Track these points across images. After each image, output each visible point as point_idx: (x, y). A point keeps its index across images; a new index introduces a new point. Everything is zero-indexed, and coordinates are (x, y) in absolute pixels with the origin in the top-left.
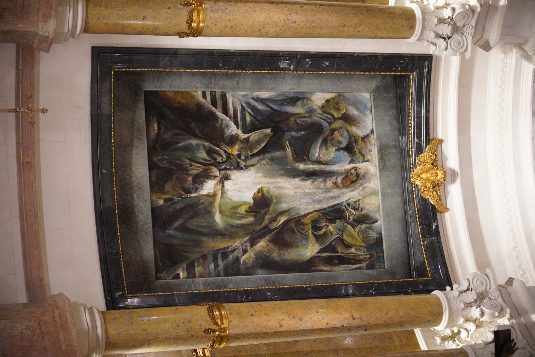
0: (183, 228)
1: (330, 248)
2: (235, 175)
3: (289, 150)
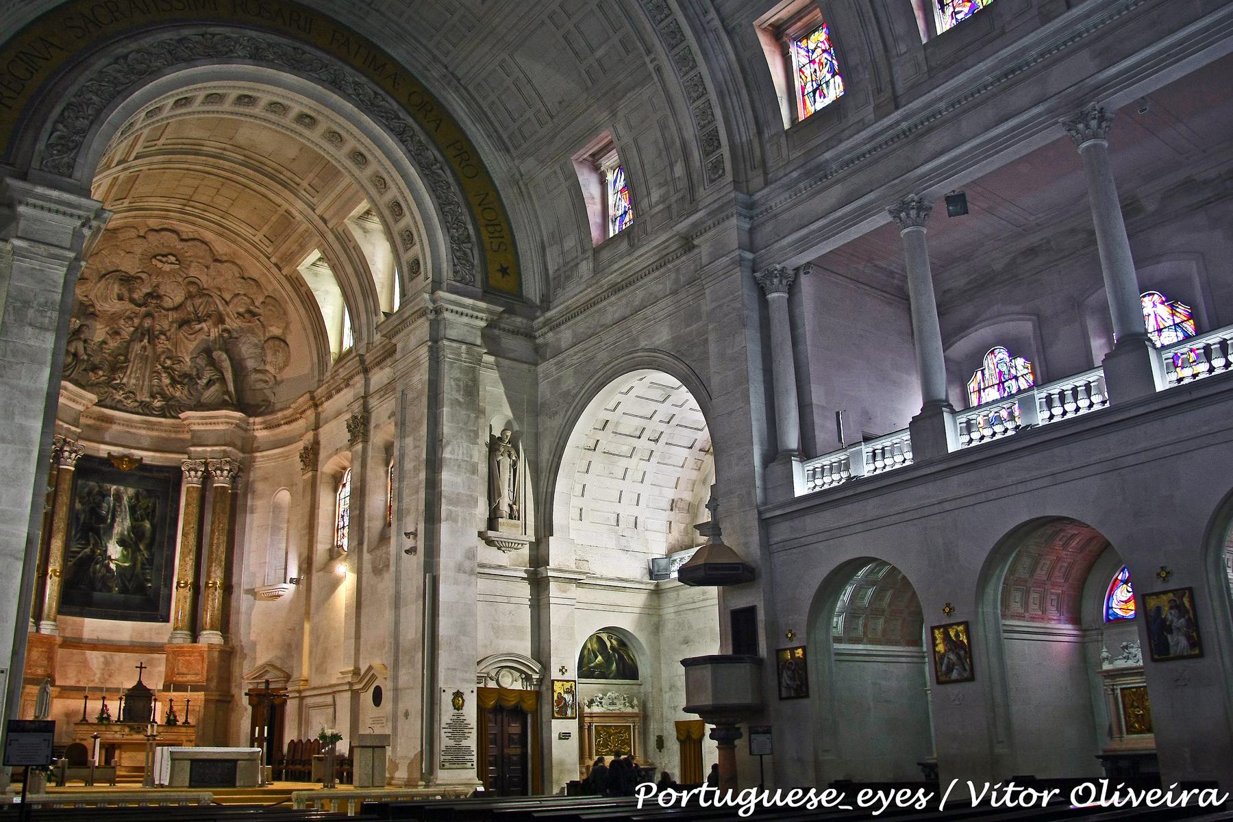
0: (129, 581)
1: (147, 515)
2: (109, 553)
3: (101, 526)
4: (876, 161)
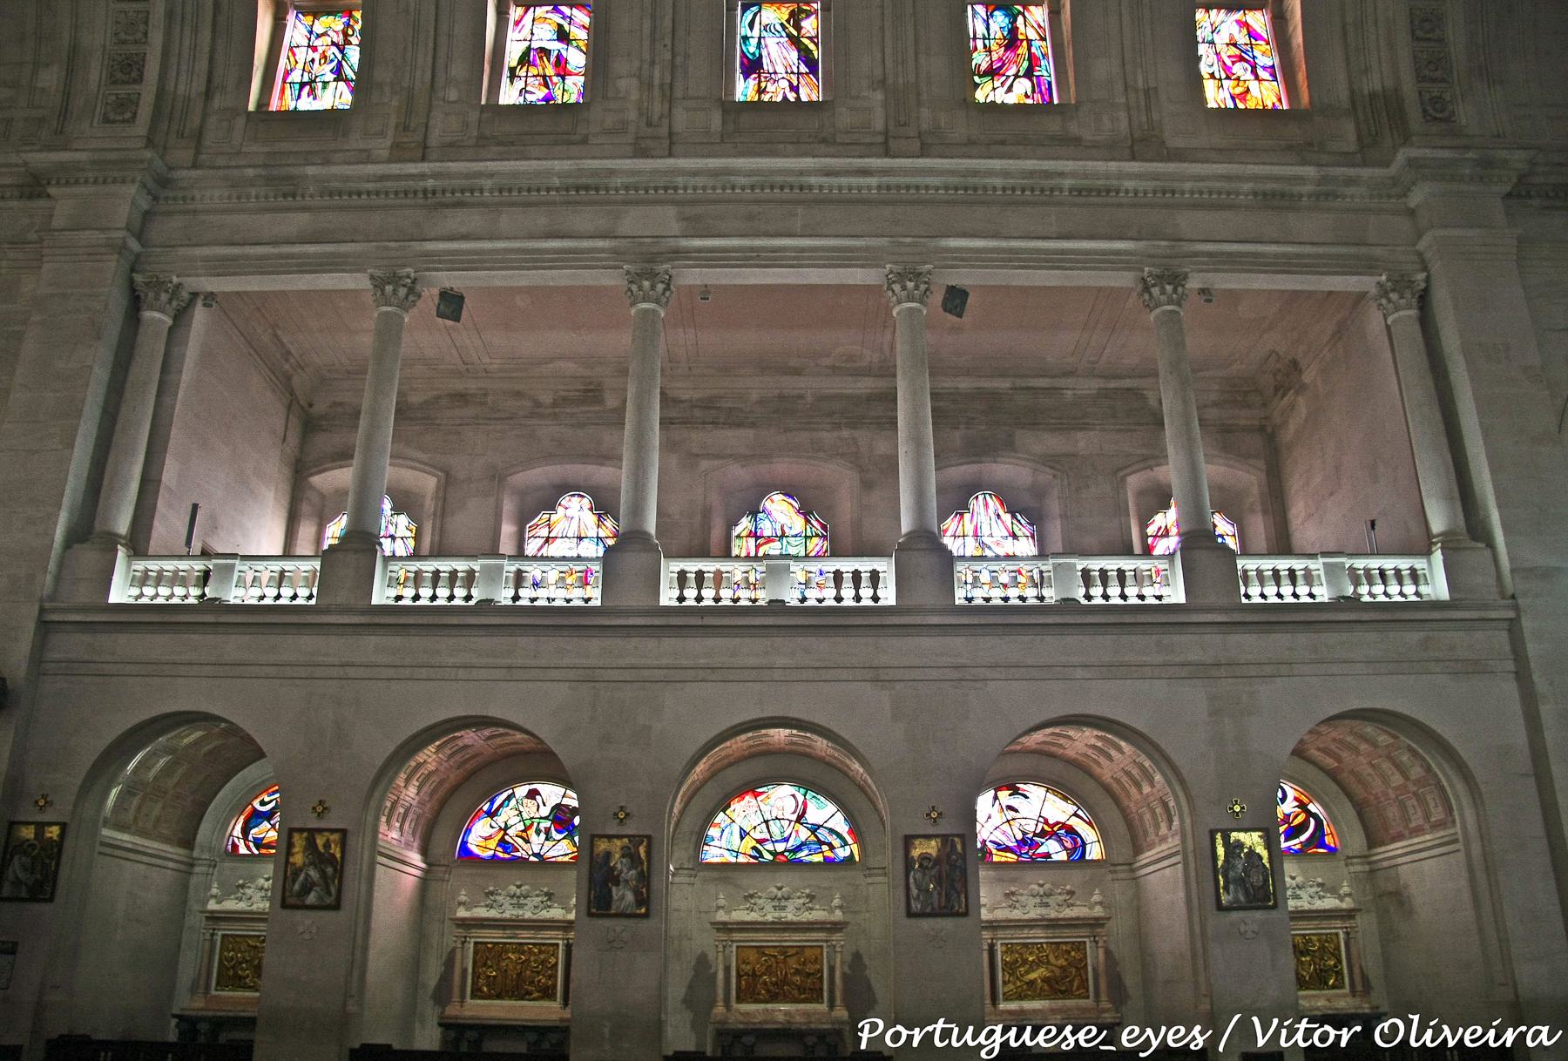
4: (371, 208)
